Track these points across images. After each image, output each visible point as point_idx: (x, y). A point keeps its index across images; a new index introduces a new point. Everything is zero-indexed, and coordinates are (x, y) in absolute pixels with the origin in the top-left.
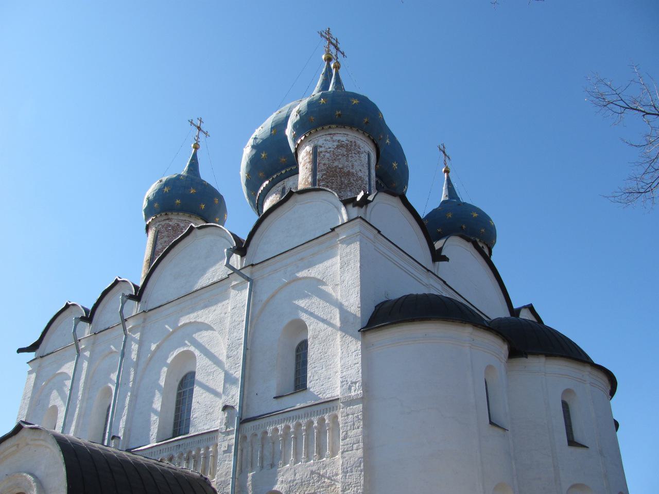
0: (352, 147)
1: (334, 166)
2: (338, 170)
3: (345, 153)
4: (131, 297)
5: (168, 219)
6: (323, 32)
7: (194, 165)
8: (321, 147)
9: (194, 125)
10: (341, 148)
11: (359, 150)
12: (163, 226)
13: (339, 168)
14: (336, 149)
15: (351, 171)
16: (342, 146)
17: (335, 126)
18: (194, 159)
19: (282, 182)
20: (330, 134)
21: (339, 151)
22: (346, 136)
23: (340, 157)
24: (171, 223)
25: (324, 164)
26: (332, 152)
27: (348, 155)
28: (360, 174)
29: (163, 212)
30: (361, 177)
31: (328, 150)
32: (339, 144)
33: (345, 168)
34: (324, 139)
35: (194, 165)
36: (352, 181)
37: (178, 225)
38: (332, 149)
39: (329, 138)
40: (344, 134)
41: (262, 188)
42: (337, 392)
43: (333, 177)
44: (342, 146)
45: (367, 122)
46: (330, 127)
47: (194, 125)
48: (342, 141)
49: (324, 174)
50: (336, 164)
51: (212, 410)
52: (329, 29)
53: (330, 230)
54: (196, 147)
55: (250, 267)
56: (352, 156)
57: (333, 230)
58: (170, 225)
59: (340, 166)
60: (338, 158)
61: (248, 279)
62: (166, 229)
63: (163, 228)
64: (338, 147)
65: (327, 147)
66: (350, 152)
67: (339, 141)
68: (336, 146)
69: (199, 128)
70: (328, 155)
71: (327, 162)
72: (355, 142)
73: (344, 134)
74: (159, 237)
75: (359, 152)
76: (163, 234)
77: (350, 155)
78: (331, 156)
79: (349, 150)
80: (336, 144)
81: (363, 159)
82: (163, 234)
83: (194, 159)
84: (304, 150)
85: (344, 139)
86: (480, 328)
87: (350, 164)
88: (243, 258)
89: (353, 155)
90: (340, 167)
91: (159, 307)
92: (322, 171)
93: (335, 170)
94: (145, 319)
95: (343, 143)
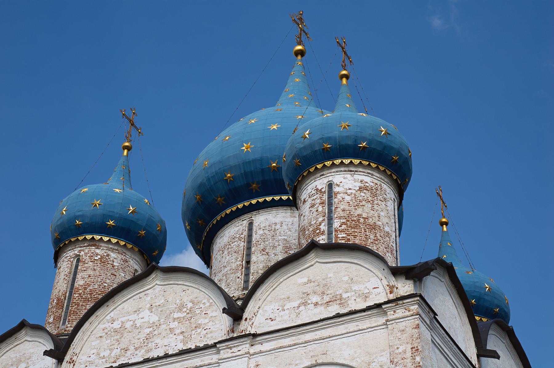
0: (378, 192)
1: (356, 215)
2: (362, 220)
3: (370, 199)
8: (338, 185)
10: (365, 191)
11: (385, 195)
13: (363, 218)
14: (359, 192)
15: (379, 223)
16: (366, 188)
19: (249, 215)
21: (363, 194)
23: (364, 203)
26: (353, 196)
28: (387, 229)
30: (388, 233)
31: (349, 191)
32: (363, 185)
33: (371, 219)
36: (379, 237)
37: (108, 255)
38: (354, 192)
39: (348, 176)
43: (355, 228)
44: (366, 188)
48: (366, 182)
49: (343, 223)
50: (359, 211)
55: (251, 337)
58: (97, 255)
59: (364, 215)
60: (361, 204)
63: (86, 255)
65: (347, 187)
68: (358, 188)
70: (348, 198)
71: (347, 208)
74: (79, 268)
76: (86, 265)
77: (376, 202)
79: (374, 195)
80: (359, 184)
87: (376, 215)
89: (380, 202)
90: (363, 216)
92: (340, 218)
93: (358, 220)
95: (367, 184)
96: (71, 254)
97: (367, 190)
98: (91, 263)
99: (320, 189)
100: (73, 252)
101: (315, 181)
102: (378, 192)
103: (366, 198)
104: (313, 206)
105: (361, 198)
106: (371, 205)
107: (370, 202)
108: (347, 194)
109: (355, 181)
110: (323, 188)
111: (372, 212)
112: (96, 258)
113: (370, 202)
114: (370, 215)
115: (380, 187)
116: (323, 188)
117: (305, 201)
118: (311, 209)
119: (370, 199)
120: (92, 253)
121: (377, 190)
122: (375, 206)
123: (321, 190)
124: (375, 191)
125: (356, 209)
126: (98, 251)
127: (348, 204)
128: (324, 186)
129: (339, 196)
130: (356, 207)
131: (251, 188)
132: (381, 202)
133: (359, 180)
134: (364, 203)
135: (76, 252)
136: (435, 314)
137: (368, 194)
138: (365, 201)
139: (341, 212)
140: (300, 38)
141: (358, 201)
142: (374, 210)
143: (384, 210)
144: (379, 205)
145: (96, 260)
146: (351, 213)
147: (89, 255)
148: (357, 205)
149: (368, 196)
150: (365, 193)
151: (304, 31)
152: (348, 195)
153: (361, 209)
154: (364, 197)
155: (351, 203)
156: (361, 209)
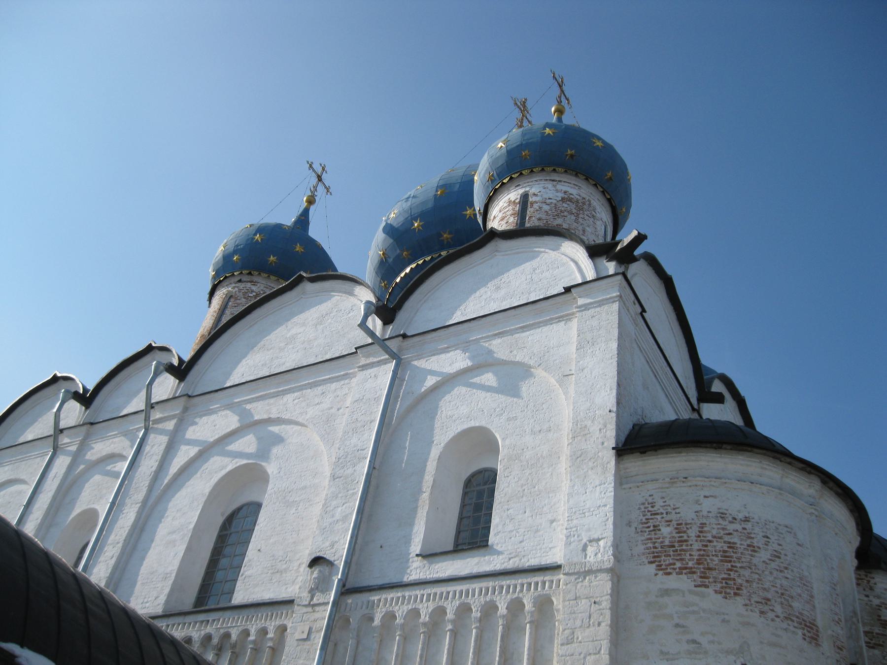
0: (585, 207)
3: (574, 211)
4: (171, 369)
5: (251, 282)
6: (518, 100)
7: (303, 220)
9: (314, 170)
10: (568, 202)
11: (593, 213)
12: (240, 290)
14: (561, 202)
16: (570, 200)
17: (563, 170)
18: (305, 213)
20: (553, 181)
21: (564, 205)
22: (577, 188)
23: (566, 214)
24: (254, 288)
25: (539, 219)
27: (578, 215)
29: (245, 269)
31: (548, 201)
32: (566, 196)
34: (543, 185)
35: (303, 220)
38: (554, 201)
40: (574, 184)
41: (402, 275)
42: (557, 556)
44: (570, 200)
45: (611, 178)
46: (554, 170)
47: (314, 170)
48: (571, 194)
51: (284, 566)
52: (526, 100)
53: (564, 291)
54: (311, 201)
55: (401, 338)
56: (584, 218)
57: (568, 290)
58: (252, 291)
61: (393, 355)
62: (244, 294)
64: (563, 200)
66: (581, 212)
67: (565, 192)
68: (560, 199)
69: (320, 178)
71: (544, 216)
72: (589, 201)
73: (574, 184)
74: (230, 303)
75: (593, 216)
76: (238, 301)
77: (581, 216)
78: (551, 210)
80: (560, 195)
81: (599, 229)
82: (238, 301)
83: (305, 213)
84: (507, 198)
85: (574, 192)
86: (831, 489)
87: (580, 228)
88: (387, 326)
89: (586, 217)
91: (217, 391)
94: (186, 409)
95: (572, 197)
96: (225, 291)
97: (571, 202)
98: (244, 300)
99: (513, 200)
100: (227, 289)
101: (508, 195)
102: (585, 207)
103: (569, 208)
104: (502, 219)
105: (563, 209)
106: (575, 218)
107: (573, 214)
108: (545, 204)
109: (557, 191)
110: (517, 199)
111: (576, 224)
112: (250, 295)
113: (573, 214)
114: (573, 227)
115: (588, 202)
116: (517, 199)
117: (495, 217)
118: (500, 222)
119: (574, 211)
120: (247, 290)
121: (584, 203)
122: (580, 220)
123: (514, 201)
124: (581, 204)
125: (555, 219)
126: (254, 288)
127: (546, 213)
128: (519, 197)
129: (536, 206)
130: (556, 217)
131: (442, 238)
132: (588, 217)
133: (563, 191)
134: (566, 214)
135: (230, 289)
136: (644, 310)
137: (573, 206)
138: (568, 212)
139: (536, 221)
140: (522, 122)
141: (559, 211)
142: (578, 223)
143: (591, 227)
144: (585, 220)
145: (250, 297)
146: (549, 223)
147: (243, 291)
148: (557, 215)
149: (572, 208)
150: (568, 204)
151: (526, 118)
152: (546, 204)
153: (562, 220)
154: (567, 207)
155: (550, 212)
156: (562, 220)
